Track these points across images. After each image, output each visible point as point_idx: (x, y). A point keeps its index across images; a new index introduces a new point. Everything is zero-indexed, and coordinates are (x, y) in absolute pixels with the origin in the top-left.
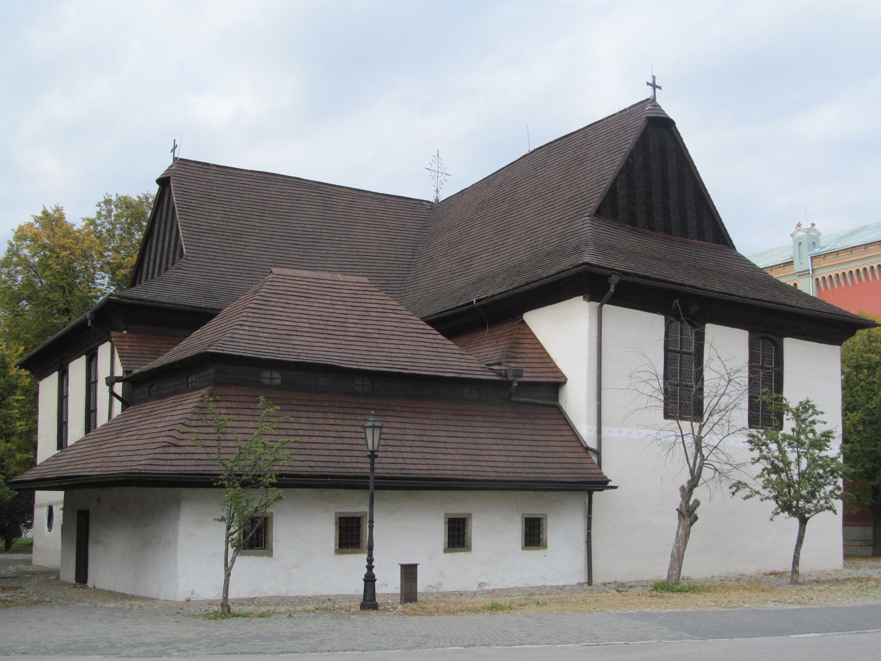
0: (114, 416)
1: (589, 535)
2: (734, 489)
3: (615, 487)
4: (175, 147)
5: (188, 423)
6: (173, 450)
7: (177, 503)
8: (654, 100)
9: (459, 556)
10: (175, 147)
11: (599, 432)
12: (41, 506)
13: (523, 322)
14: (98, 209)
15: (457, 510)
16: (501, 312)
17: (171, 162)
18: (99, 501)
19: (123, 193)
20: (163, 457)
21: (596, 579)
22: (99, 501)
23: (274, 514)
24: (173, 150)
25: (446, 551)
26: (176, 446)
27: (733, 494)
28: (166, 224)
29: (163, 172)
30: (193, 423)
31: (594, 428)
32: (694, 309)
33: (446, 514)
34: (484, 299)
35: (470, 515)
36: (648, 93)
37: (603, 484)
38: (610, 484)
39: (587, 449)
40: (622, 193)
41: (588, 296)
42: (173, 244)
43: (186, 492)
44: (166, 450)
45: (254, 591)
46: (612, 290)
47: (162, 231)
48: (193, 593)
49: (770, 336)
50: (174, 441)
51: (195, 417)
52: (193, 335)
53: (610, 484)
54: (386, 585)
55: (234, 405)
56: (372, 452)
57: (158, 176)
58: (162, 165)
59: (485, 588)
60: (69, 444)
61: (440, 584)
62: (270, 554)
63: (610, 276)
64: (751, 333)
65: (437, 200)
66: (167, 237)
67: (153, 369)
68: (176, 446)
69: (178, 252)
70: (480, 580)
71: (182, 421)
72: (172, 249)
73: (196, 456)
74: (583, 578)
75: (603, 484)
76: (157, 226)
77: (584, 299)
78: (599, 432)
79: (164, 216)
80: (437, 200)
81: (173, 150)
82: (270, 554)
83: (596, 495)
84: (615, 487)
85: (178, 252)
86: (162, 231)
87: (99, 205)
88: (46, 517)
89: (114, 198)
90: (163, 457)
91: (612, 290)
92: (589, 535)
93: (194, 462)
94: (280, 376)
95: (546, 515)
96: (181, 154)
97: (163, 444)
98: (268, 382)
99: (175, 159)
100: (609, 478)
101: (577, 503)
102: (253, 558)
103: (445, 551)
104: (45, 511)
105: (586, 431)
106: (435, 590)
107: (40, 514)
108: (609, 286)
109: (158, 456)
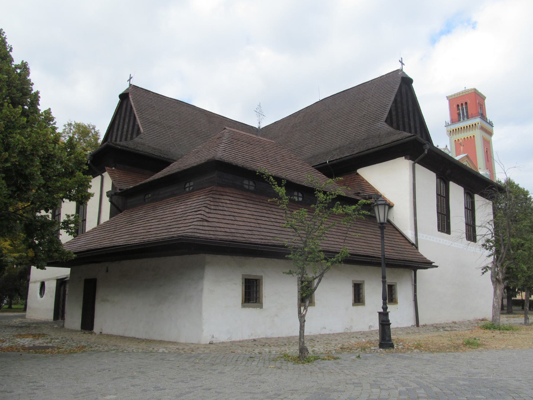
0: (102, 222)
1: (415, 296)
2: (484, 270)
3: (437, 267)
4: (131, 78)
5: (209, 206)
6: (206, 224)
7: (201, 266)
8: (402, 70)
9: (359, 308)
10: (131, 78)
11: (416, 235)
12: (35, 282)
13: (357, 174)
14: (64, 128)
15: (358, 279)
16: (345, 167)
17: (128, 86)
18: (107, 271)
19: (78, 122)
20: (201, 228)
21: (421, 323)
22: (107, 271)
23: (263, 277)
24: (129, 80)
25: (353, 305)
26: (207, 221)
27: (483, 273)
28: (124, 120)
29: (123, 91)
30: (212, 207)
31: (413, 233)
32: (449, 171)
33: (353, 281)
34: (333, 160)
35: (364, 281)
36: (398, 67)
37: (427, 264)
38: (433, 264)
39: (413, 244)
40: (394, 113)
41: (408, 156)
42: (131, 128)
43: (208, 257)
44: (201, 223)
45: (252, 335)
46: (426, 152)
47: (121, 124)
48: (213, 337)
49: (470, 192)
50: (204, 218)
51: (212, 203)
52: (171, 166)
53: (433, 264)
54: (325, 328)
55: (233, 199)
56: (382, 224)
57: (121, 93)
58: (123, 88)
59: (372, 329)
60: (86, 231)
61: (351, 327)
62: (261, 307)
63: (425, 144)
64: (465, 189)
65: (259, 127)
66: (126, 126)
67: (162, 178)
68: (207, 221)
69: (135, 131)
70: (370, 325)
71: (205, 205)
72: (130, 132)
73: (223, 230)
74: (413, 322)
75: (427, 264)
76: (117, 122)
77: (406, 158)
78: (416, 235)
79: (123, 115)
80: (259, 127)
81: (129, 80)
82: (261, 307)
83: (419, 271)
84: (437, 267)
85: (135, 131)
86: (121, 124)
87: (65, 126)
88: (39, 289)
89: (73, 123)
90: (201, 228)
91: (426, 152)
92: (415, 296)
93: (224, 234)
94: (254, 185)
95: (396, 283)
96: (134, 82)
97: (200, 219)
98: (247, 187)
99: (130, 85)
100: (432, 261)
101: (408, 276)
102: (251, 309)
103: (353, 305)
104: (38, 285)
105: (410, 234)
106: (349, 331)
107: (34, 288)
108: (424, 151)
109: (198, 227)
